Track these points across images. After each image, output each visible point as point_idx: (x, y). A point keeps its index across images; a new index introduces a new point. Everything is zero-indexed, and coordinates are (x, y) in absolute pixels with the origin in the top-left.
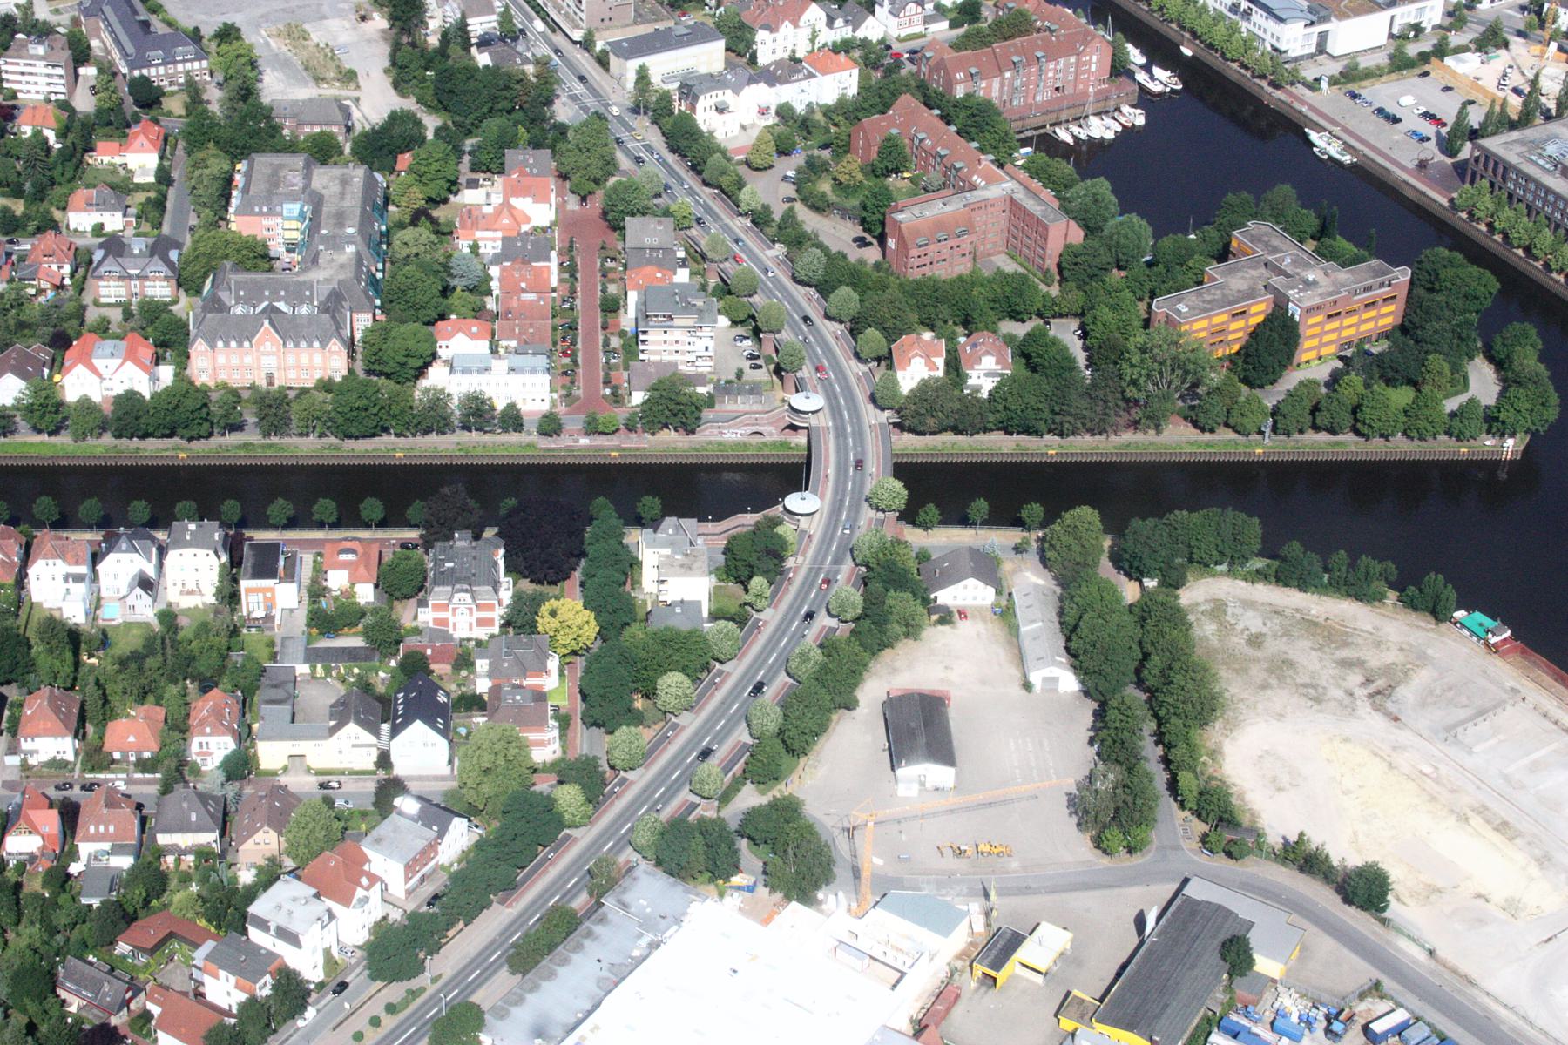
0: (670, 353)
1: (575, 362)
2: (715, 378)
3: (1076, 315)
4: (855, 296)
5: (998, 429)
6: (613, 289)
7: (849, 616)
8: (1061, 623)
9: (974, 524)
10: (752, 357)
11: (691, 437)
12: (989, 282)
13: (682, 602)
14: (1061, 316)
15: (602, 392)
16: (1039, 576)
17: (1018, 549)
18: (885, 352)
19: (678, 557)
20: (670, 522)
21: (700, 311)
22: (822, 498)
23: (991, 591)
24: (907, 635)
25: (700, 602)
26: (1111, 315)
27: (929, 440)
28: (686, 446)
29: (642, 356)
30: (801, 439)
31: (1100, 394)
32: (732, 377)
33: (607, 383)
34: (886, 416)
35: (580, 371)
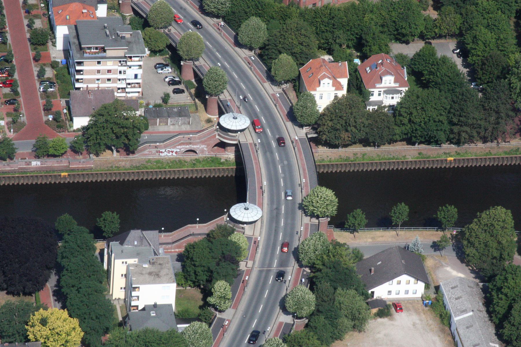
0: (103, 81)
1: (16, 93)
2: (144, 102)
3: (452, 36)
4: (263, 25)
5: (401, 141)
6: (38, 24)
7: (304, 313)
8: (489, 312)
9: (396, 226)
10: (173, 82)
11: (131, 156)
12: (378, 8)
13: (155, 306)
14: (440, 37)
15: (45, 119)
16: (459, 271)
17: (436, 246)
18: (294, 75)
19: (146, 266)
20: (134, 234)
21: (129, 43)
22: (261, 206)
23: (421, 286)
24: (354, 327)
25: (171, 304)
26: (489, 35)
27: (341, 152)
28: (128, 165)
29: (77, 85)
30: (230, 155)
31: (493, 105)
32: (159, 101)
33: (47, 109)
34: (304, 132)
35: (21, 99)
